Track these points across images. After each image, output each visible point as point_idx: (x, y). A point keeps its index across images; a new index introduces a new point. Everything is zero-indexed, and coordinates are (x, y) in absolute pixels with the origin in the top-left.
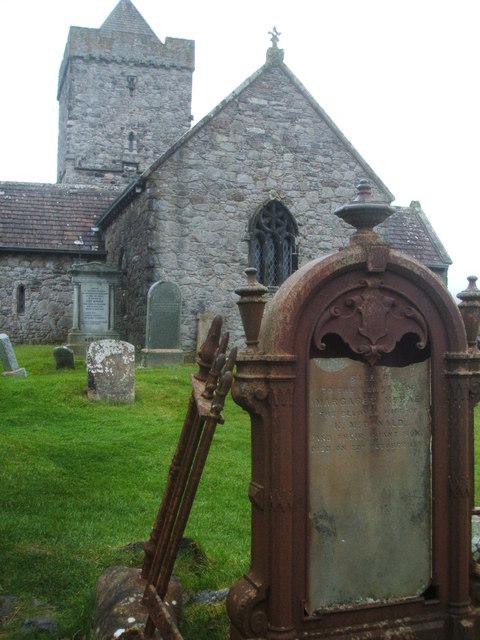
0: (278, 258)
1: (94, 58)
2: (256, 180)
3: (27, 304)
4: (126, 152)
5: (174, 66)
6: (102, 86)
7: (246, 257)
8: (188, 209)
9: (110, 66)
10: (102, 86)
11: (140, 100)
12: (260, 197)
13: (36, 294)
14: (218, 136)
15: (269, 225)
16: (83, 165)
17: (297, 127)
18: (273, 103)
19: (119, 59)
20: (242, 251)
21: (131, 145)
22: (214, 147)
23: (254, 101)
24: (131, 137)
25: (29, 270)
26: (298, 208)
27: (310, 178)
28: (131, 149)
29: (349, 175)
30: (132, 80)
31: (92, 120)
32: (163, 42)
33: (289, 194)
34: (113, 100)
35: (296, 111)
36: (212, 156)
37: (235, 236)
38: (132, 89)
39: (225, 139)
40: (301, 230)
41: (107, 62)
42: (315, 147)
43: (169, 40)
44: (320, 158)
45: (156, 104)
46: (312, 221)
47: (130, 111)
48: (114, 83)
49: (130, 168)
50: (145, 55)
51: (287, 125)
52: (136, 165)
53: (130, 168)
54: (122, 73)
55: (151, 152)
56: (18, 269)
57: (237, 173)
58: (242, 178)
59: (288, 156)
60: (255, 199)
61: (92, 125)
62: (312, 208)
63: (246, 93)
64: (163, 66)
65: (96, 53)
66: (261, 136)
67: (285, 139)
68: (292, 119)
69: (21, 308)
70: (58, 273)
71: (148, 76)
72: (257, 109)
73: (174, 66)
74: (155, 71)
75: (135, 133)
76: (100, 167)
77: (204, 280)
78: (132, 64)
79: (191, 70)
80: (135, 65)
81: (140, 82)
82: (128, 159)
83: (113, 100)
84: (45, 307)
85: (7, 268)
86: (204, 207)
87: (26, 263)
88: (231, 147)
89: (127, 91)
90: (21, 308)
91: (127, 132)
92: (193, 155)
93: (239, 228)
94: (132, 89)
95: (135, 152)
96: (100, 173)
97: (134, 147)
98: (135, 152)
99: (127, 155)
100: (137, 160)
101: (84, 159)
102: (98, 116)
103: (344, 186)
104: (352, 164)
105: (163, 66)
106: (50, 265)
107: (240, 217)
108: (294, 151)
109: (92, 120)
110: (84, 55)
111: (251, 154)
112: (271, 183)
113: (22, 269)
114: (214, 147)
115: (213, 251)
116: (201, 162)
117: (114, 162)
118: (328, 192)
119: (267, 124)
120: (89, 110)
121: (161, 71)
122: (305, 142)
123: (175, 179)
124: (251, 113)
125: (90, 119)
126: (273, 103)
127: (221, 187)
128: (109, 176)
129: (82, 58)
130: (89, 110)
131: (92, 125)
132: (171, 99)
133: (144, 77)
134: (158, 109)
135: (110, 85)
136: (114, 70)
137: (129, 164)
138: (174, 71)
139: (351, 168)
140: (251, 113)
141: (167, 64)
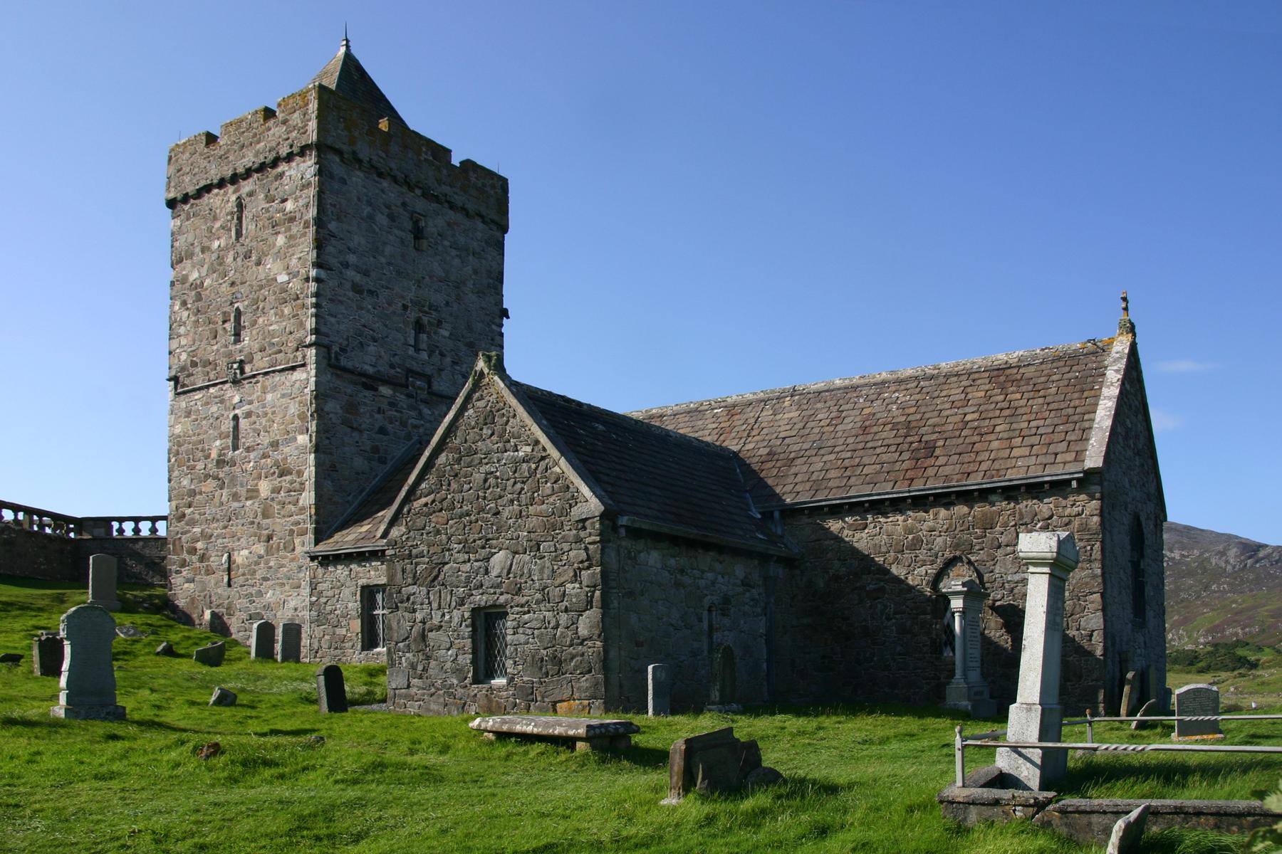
1: (360, 161)
6: (371, 218)
9: (385, 184)
10: (371, 218)
16: (344, 362)
19: (400, 176)
21: (416, 339)
24: (419, 327)
31: (358, 278)
32: (458, 165)
34: (388, 249)
41: (380, 175)
43: (468, 165)
48: (392, 218)
50: (439, 182)
52: (429, 379)
55: (448, 360)
61: (357, 289)
64: (464, 210)
73: (482, 217)
74: (451, 215)
75: (425, 320)
76: (371, 370)
78: (418, 192)
79: (505, 229)
81: (433, 226)
87: (718, 567)
89: (410, 237)
91: (412, 315)
95: (424, 355)
96: (370, 382)
97: (424, 346)
100: (428, 370)
101: (343, 350)
102: (366, 273)
105: (464, 210)
106: (740, 570)
109: (358, 278)
110: (345, 148)
117: (392, 366)
120: (352, 259)
121: (459, 217)
125: (350, 273)
128: (385, 390)
130: (352, 259)
131: (357, 289)
135: (382, 220)
136: (392, 193)
138: (480, 226)
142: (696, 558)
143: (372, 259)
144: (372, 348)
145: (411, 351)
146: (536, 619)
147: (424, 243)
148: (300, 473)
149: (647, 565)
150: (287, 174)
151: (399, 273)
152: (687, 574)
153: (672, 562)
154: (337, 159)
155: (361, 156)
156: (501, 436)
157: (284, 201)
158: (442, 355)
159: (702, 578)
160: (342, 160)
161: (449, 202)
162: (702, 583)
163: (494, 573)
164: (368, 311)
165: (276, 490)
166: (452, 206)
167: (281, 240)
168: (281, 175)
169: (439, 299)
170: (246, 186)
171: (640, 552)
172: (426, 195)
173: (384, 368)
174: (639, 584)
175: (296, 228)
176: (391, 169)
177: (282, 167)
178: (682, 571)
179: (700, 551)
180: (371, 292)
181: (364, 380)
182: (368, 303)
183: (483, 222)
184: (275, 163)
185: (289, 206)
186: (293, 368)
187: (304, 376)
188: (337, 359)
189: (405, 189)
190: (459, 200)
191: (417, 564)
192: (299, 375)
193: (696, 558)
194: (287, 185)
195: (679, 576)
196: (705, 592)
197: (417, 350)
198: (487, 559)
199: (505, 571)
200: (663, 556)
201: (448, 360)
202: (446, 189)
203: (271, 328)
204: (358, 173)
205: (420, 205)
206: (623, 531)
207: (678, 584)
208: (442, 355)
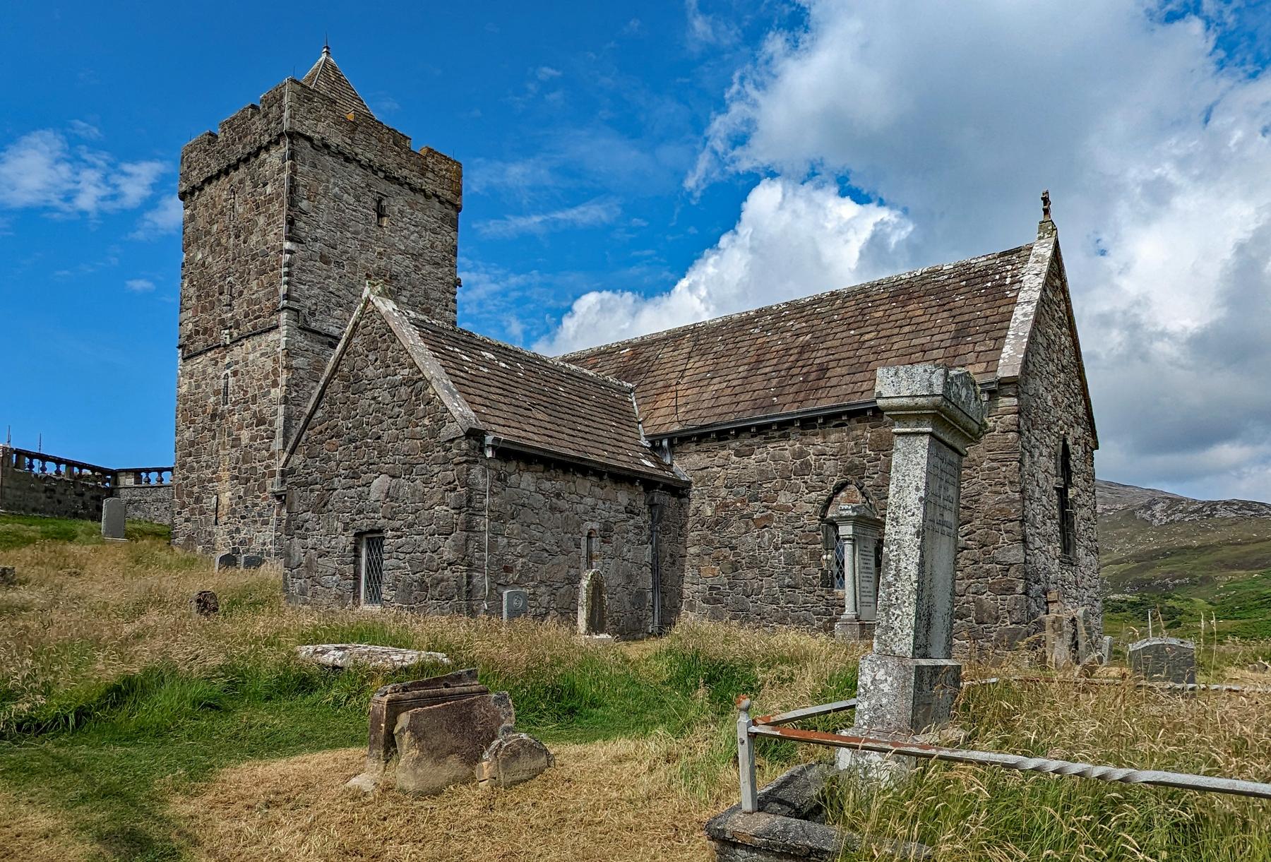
1: (327, 146)
5: (438, 197)
9: (352, 167)
10: (337, 198)
13: (607, 548)
30: (379, 202)
31: (326, 250)
38: (380, 216)
41: (347, 159)
47: (378, 250)
50: (400, 166)
65: (335, 140)
78: (381, 174)
80: (386, 178)
81: (396, 204)
94: (380, 216)
106: (623, 497)
121: (421, 199)
129: (309, 139)
131: (324, 259)
132: (432, 247)
134: (416, 257)
135: (351, 200)
136: (358, 177)
141: (429, 188)
142: (574, 482)
143: (338, 233)
146: (408, 543)
147: (385, 221)
148: (271, 423)
149: (519, 487)
150: (267, 161)
152: (564, 498)
153: (547, 485)
154: (308, 144)
155: (329, 142)
156: (382, 362)
157: (265, 185)
159: (581, 503)
160: (312, 147)
161: (409, 184)
162: (580, 508)
163: (373, 497)
164: (335, 279)
165: (253, 439)
166: (413, 189)
167: (262, 220)
168: (262, 164)
170: (236, 176)
171: (510, 475)
172: (389, 178)
174: (509, 507)
175: (275, 207)
176: (356, 154)
177: (263, 155)
178: (558, 496)
179: (578, 475)
180: (339, 265)
181: (330, 340)
182: (335, 272)
183: (440, 202)
184: (257, 155)
185: (269, 189)
186: (269, 330)
187: (277, 336)
189: (369, 172)
190: (417, 181)
191: (312, 491)
192: (272, 336)
193: (574, 482)
194: (267, 171)
195: (554, 500)
196: (584, 517)
198: (368, 484)
199: (383, 495)
200: (538, 479)
202: (405, 172)
203: (253, 297)
204: (327, 157)
205: (384, 187)
206: (489, 454)
207: (553, 509)
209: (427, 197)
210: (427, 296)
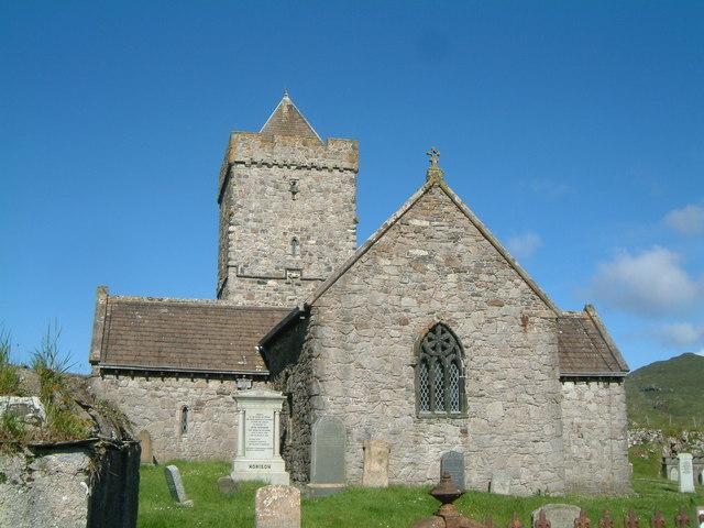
0: (445, 382)
1: (256, 163)
2: (420, 302)
3: (190, 425)
4: (289, 257)
7: (411, 382)
8: (352, 335)
11: (301, 205)
12: (425, 320)
13: (199, 416)
14: (382, 260)
15: (434, 349)
16: (246, 273)
17: (460, 246)
18: (436, 223)
19: (281, 163)
20: (408, 377)
22: (379, 271)
23: (416, 222)
25: (192, 391)
26: (464, 329)
27: (475, 298)
28: (294, 254)
29: (515, 293)
31: (254, 225)
33: (454, 315)
34: (274, 205)
35: (459, 230)
36: (376, 281)
37: (400, 361)
38: (294, 193)
39: (389, 263)
40: (466, 351)
42: (479, 266)
44: (485, 278)
45: (318, 207)
46: (479, 343)
49: (294, 275)
51: (450, 244)
53: (294, 275)
54: (284, 177)
55: (315, 257)
56: (182, 390)
57: (402, 296)
58: (406, 301)
59: (452, 277)
60: (419, 324)
61: (255, 231)
62: (478, 329)
63: (408, 215)
66: (423, 258)
67: (449, 260)
68: (455, 238)
69: (184, 429)
70: (221, 393)
71: (309, 179)
72: (418, 230)
75: (298, 238)
77: (371, 406)
81: (301, 185)
82: (293, 266)
83: (274, 205)
84: (207, 429)
85: (170, 389)
86: (369, 332)
88: (395, 271)
90: (184, 429)
91: (290, 237)
92: (356, 280)
93: (406, 354)
94: (294, 193)
95: (298, 258)
96: (262, 280)
98: (298, 258)
99: (290, 261)
103: (510, 303)
104: (518, 281)
106: (214, 384)
107: (405, 342)
108: (458, 271)
109: (254, 225)
111: (415, 276)
112: (436, 305)
113: (185, 390)
114: (379, 271)
115: (378, 377)
116: (365, 287)
117: (277, 268)
118: (495, 311)
119: (430, 245)
120: (251, 216)
121: (324, 173)
122: (467, 262)
123: (339, 305)
124: (413, 235)
126: (436, 223)
127: (386, 311)
131: (255, 231)
132: (335, 201)
133: (305, 180)
134: (322, 212)
137: (291, 270)
139: (517, 285)
140: (413, 235)
144: (264, 261)
145: (289, 257)
147: (297, 196)
151: (281, 216)
158: (310, 255)
169: (303, 223)
173: (272, 271)
178: (157, 389)
188: (242, 271)
197: (294, 254)
201: (315, 257)
205: (295, 174)
207: (153, 396)
208: (310, 255)
209: (330, 171)
210: (331, 236)
